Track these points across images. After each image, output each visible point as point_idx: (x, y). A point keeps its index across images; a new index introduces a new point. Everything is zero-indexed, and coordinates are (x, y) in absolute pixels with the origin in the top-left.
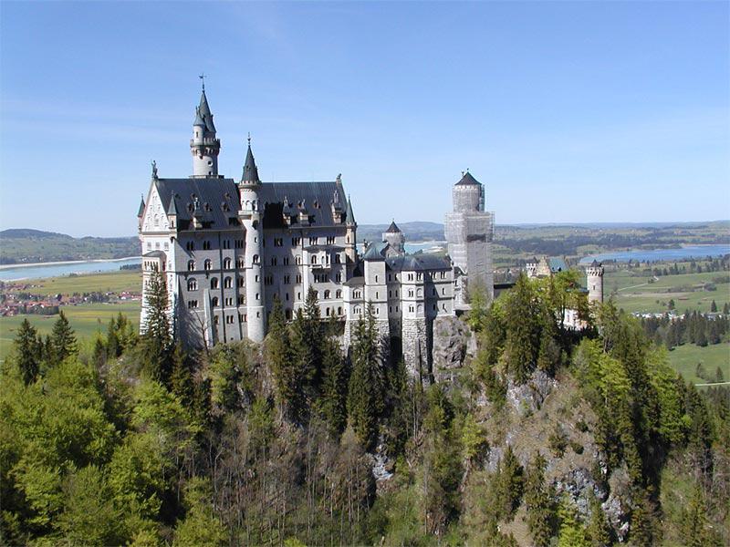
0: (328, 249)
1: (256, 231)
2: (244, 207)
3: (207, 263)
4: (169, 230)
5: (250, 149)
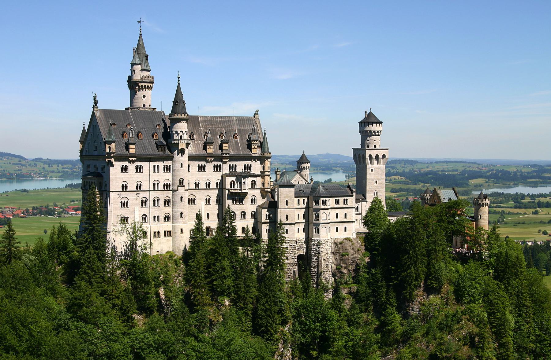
3: (139, 187)
5: (179, 83)
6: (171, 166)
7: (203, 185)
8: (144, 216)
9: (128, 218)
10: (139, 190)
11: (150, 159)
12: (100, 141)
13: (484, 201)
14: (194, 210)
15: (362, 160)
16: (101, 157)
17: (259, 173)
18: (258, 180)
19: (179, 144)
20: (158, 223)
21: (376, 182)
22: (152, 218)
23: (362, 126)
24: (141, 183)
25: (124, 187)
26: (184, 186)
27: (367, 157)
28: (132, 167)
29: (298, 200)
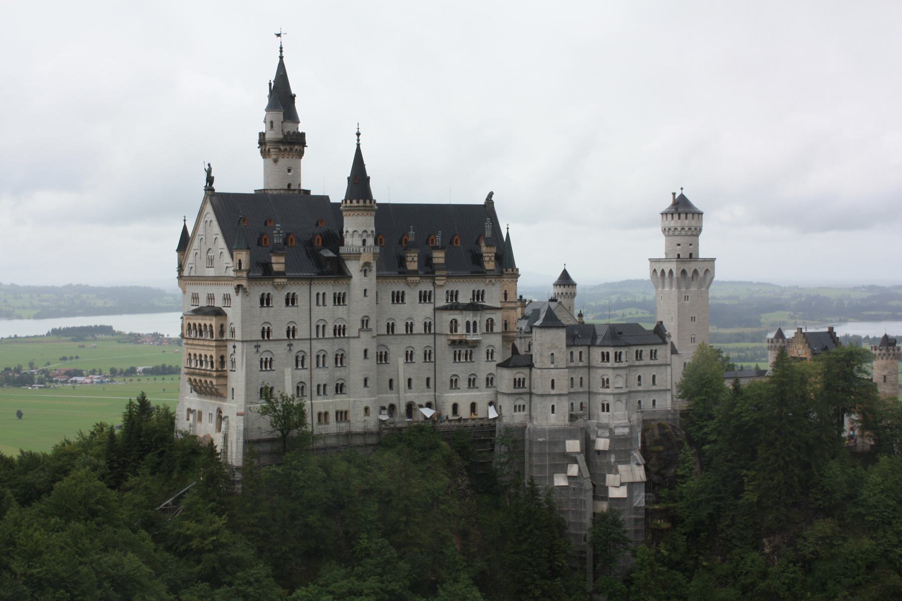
0: (475, 307)
1: (366, 280)
2: (348, 240)
3: (291, 332)
4: (232, 274)
5: (358, 145)
6: (347, 294)
7: (400, 329)
8: (300, 386)
10: (291, 337)
11: (310, 280)
12: (220, 251)
13: (891, 351)
14: (388, 371)
15: (667, 281)
16: (221, 279)
17: (499, 305)
18: (497, 317)
19: (360, 254)
20: (325, 397)
21: (693, 319)
22: (315, 389)
23: (667, 220)
24: (294, 325)
25: (266, 333)
26: (371, 330)
28: (278, 298)
29: (572, 353)
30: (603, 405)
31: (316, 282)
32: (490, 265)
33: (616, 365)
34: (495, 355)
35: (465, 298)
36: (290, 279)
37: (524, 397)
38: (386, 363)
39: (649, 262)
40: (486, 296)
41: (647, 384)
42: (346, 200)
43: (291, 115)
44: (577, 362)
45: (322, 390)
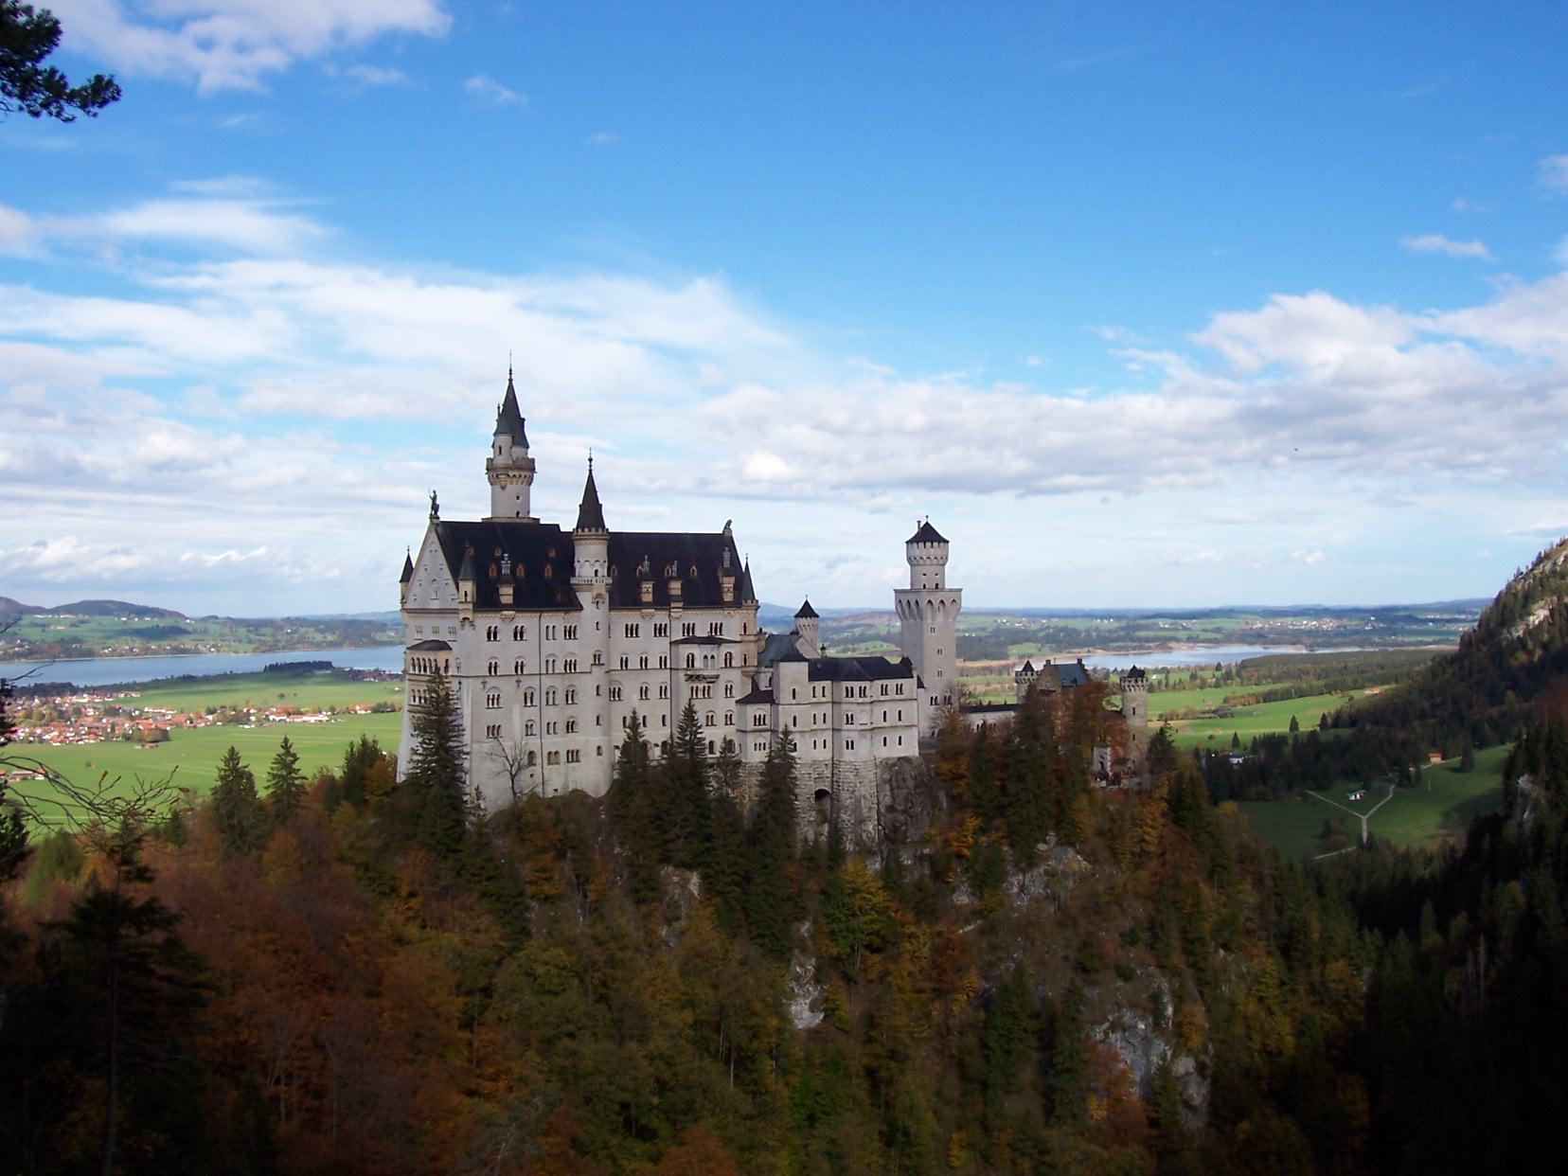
3: (519, 667)
4: (461, 607)
5: (590, 471)
7: (634, 664)
8: (529, 724)
9: (499, 727)
10: (519, 672)
17: (738, 640)
18: (736, 651)
21: (940, 652)
22: (545, 727)
25: (493, 669)
27: (923, 604)
28: (506, 632)
29: (814, 688)
30: (847, 742)
31: (546, 614)
32: (728, 597)
33: (861, 700)
34: (734, 690)
35: (702, 631)
36: (517, 611)
37: (763, 734)
38: (620, 700)
39: (893, 593)
40: (723, 628)
41: (892, 719)
42: (577, 528)
43: (520, 439)
44: (819, 698)
45: (551, 728)
